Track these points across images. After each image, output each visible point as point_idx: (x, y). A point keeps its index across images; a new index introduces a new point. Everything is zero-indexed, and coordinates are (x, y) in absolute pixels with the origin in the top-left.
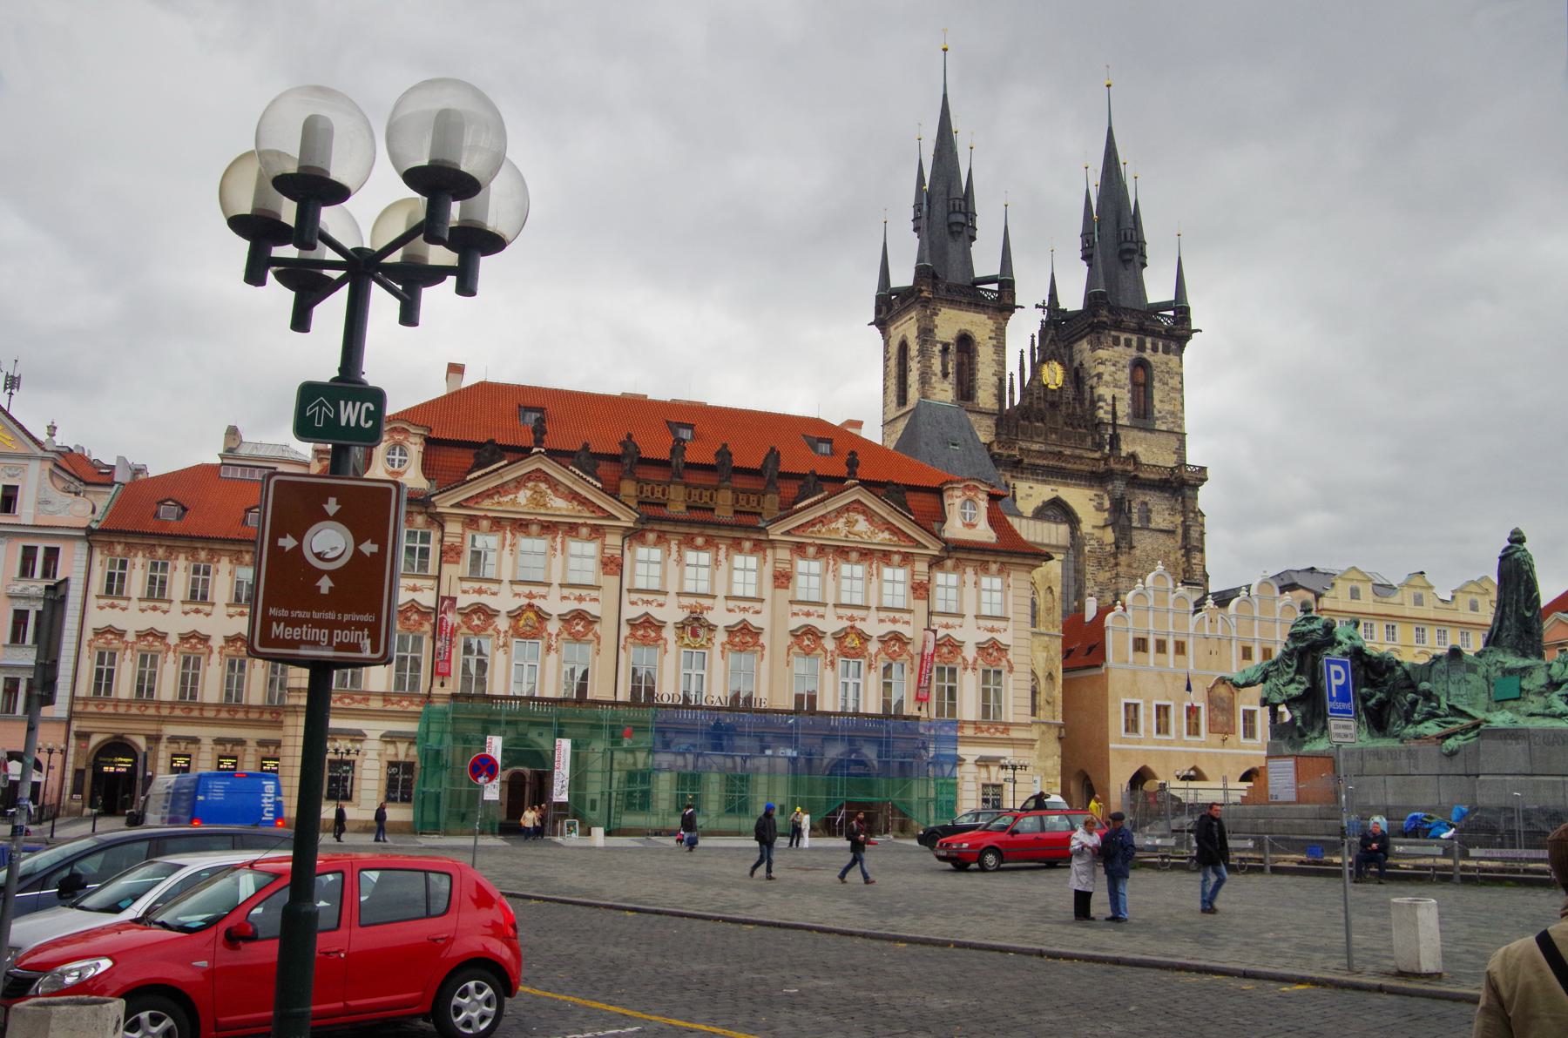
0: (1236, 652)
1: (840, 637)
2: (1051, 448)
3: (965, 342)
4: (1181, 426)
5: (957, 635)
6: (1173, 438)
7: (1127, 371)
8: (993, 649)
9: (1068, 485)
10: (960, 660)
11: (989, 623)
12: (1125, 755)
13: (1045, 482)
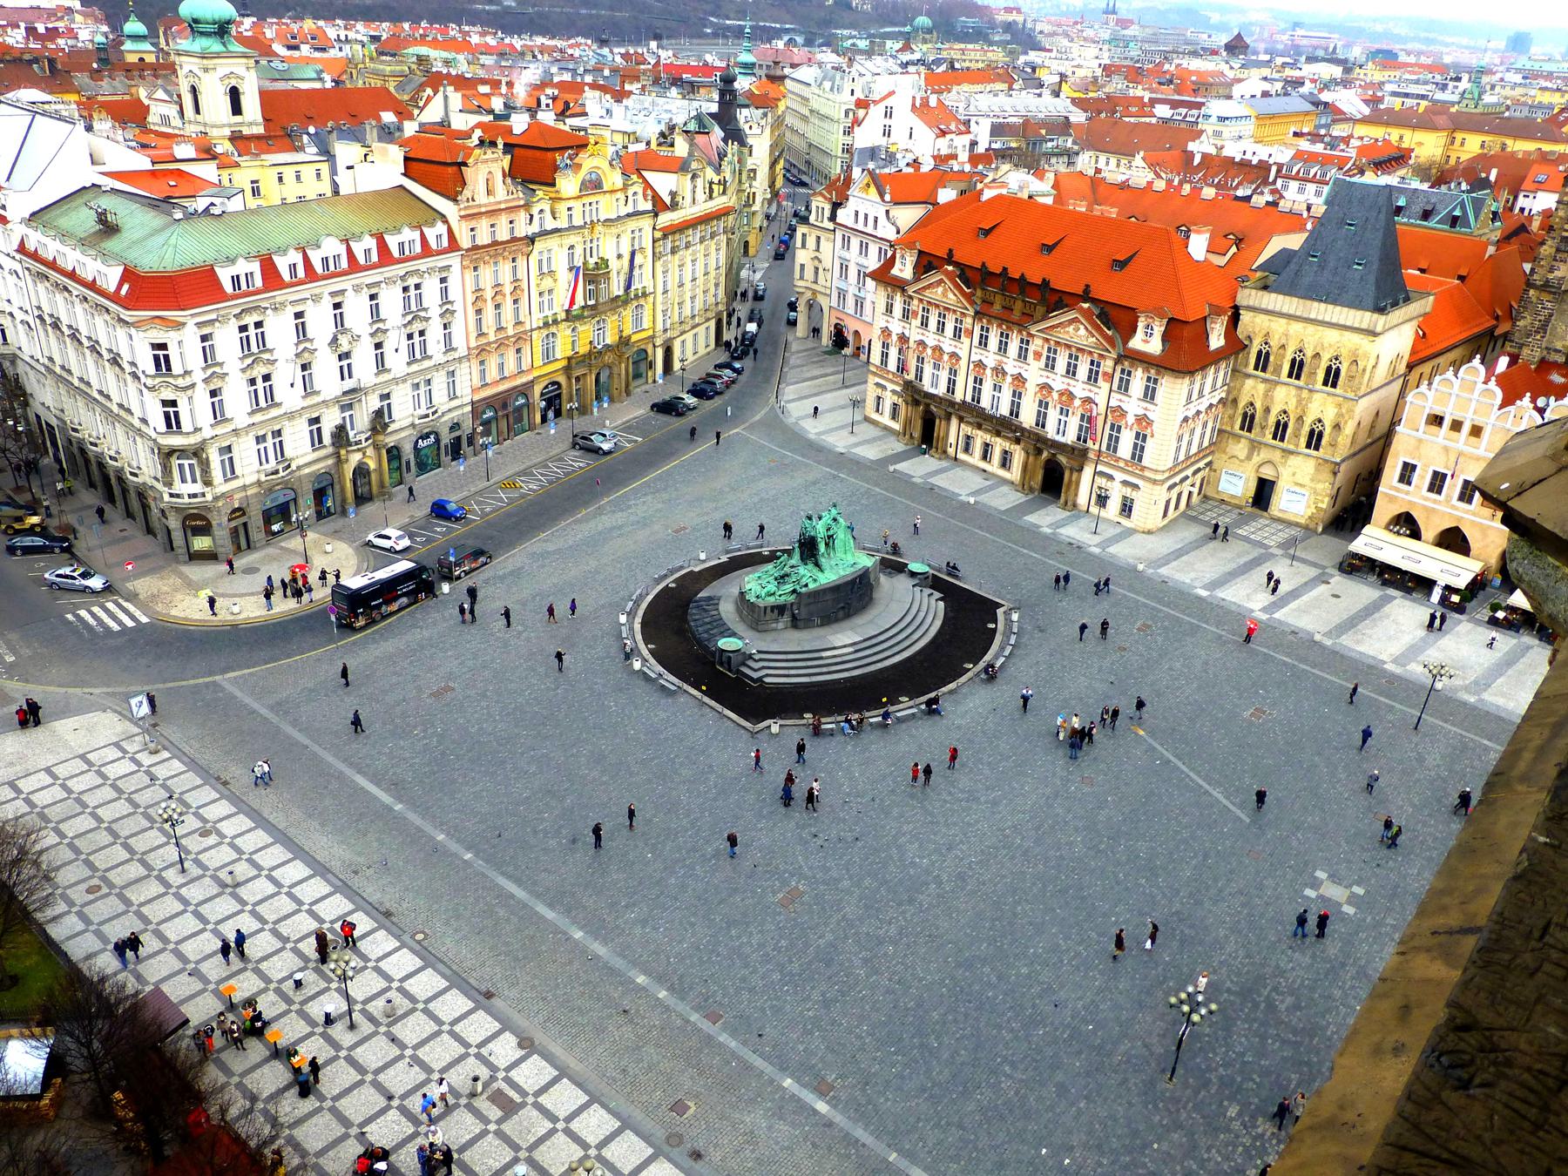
1: (1061, 394)
8: (1142, 420)
12: (1392, 499)
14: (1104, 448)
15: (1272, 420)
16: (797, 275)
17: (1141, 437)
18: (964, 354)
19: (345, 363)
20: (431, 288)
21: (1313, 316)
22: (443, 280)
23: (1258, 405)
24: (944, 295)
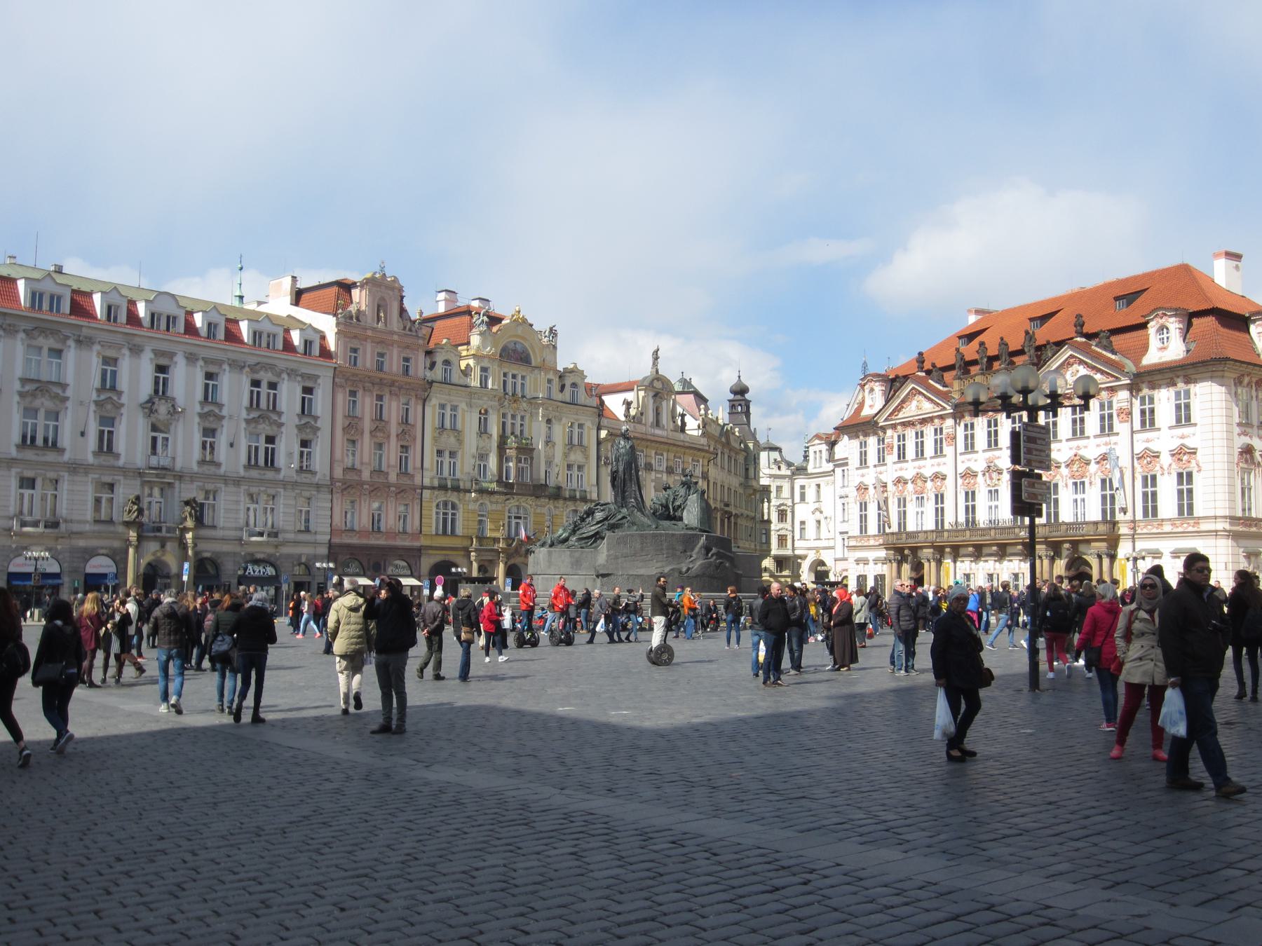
5: (1154, 446)
8: (1181, 453)
10: (1158, 468)
11: (1180, 431)
14: (1139, 515)
17: (1185, 478)
18: (948, 470)
19: (160, 436)
20: (289, 396)
22: (308, 390)
24: (918, 408)
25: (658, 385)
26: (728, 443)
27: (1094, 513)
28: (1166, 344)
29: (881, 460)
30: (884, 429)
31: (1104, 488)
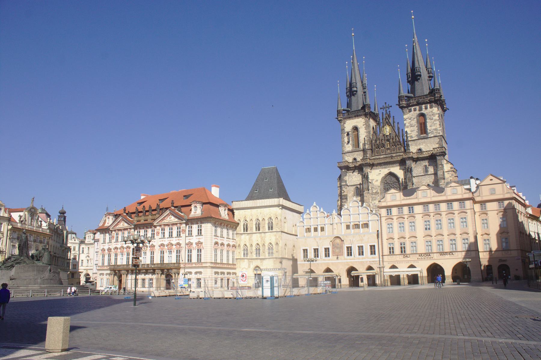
0: (344, 226)
2: (387, 156)
3: (356, 129)
4: (439, 133)
6: (437, 138)
7: (415, 119)
8: (199, 243)
9: (393, 167)
13: (385, 168)
14: (187, 262)
15: (254, 248)
16: (80, 264)
17: (199, 251)
21: (258, 205)
23: (248, 245)
25: (33, 210)
26: (57, 231)
27: (174, 261)
28: (197, 211)
29: (110, 242)
30: (112, 231)
31: (177, 253)
